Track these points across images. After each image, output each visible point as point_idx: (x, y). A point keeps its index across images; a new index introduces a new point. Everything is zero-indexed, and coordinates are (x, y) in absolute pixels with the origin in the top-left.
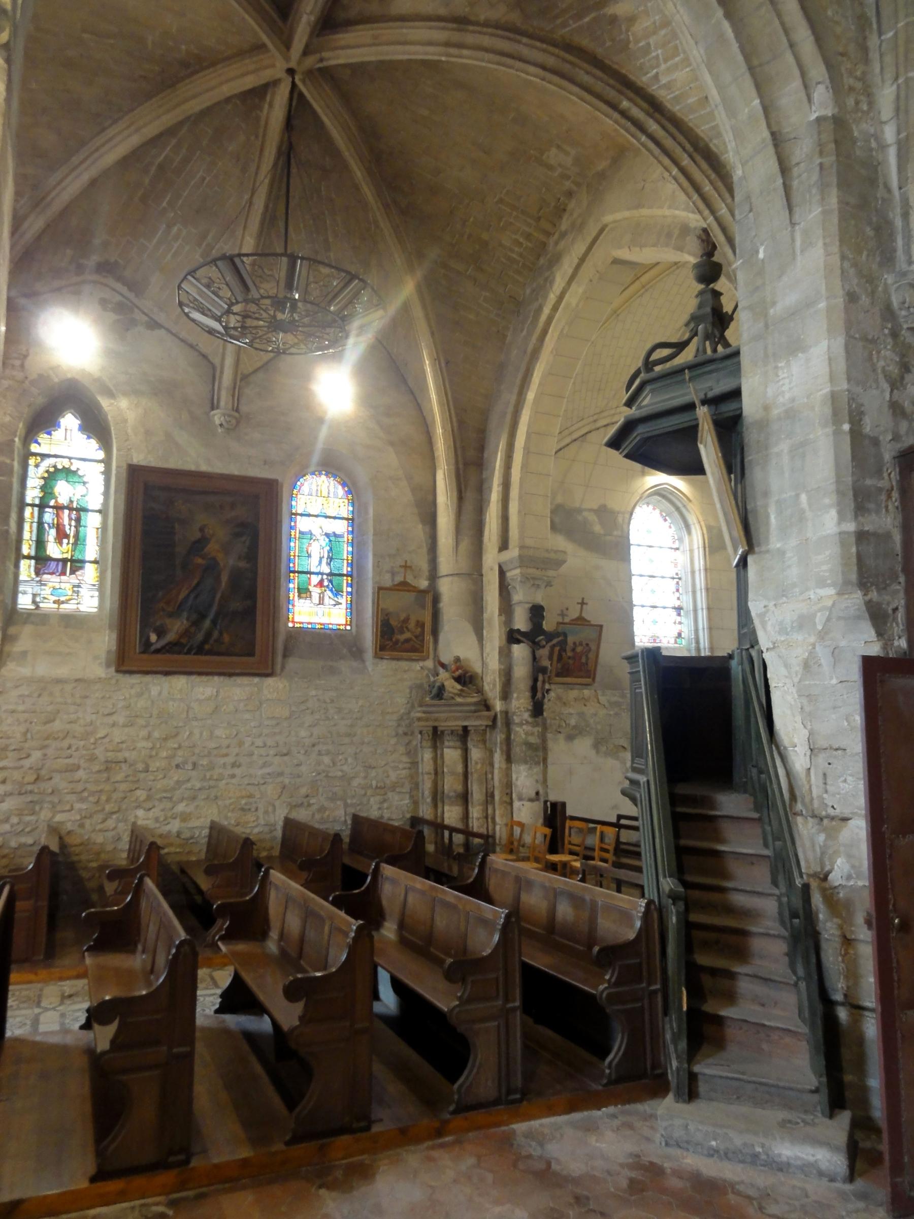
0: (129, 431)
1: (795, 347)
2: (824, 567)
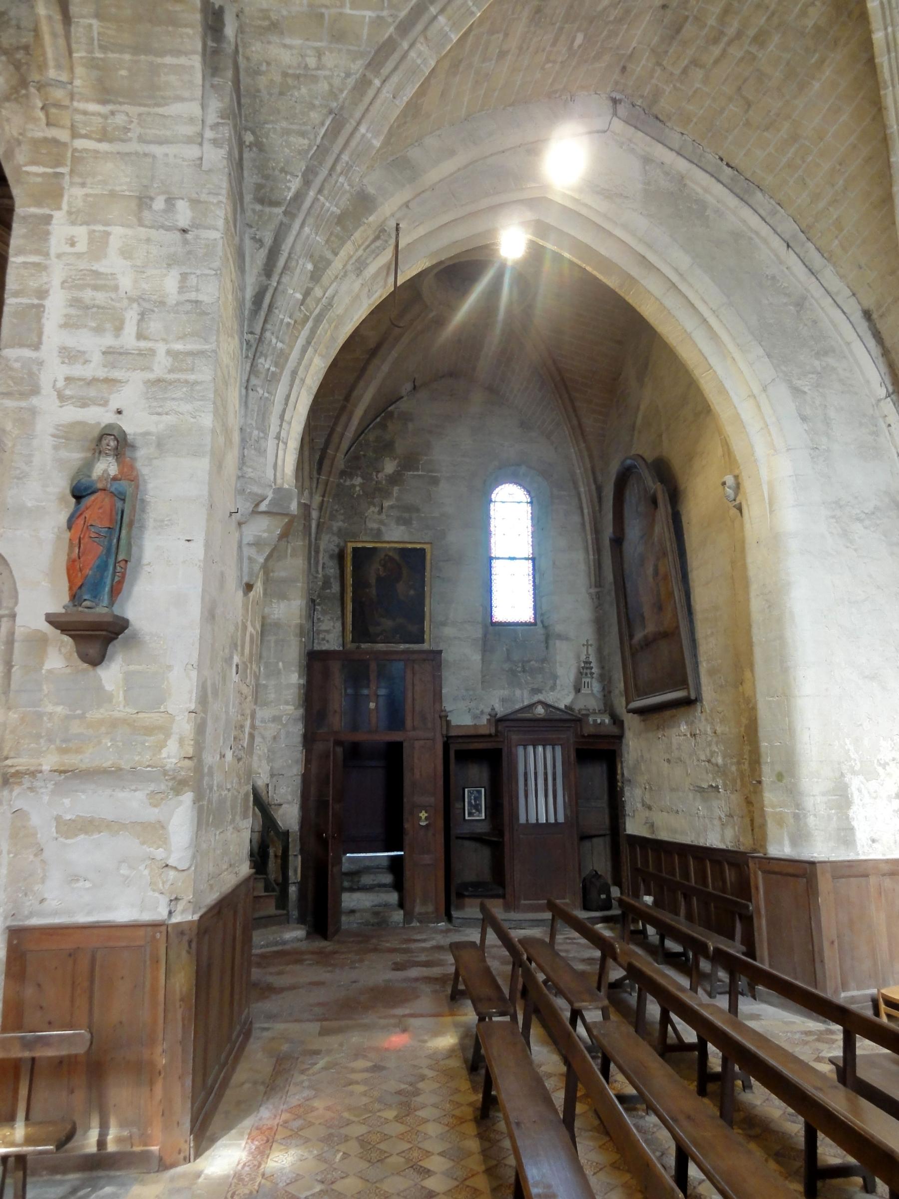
1: (283, 597)
2: (289, 697)
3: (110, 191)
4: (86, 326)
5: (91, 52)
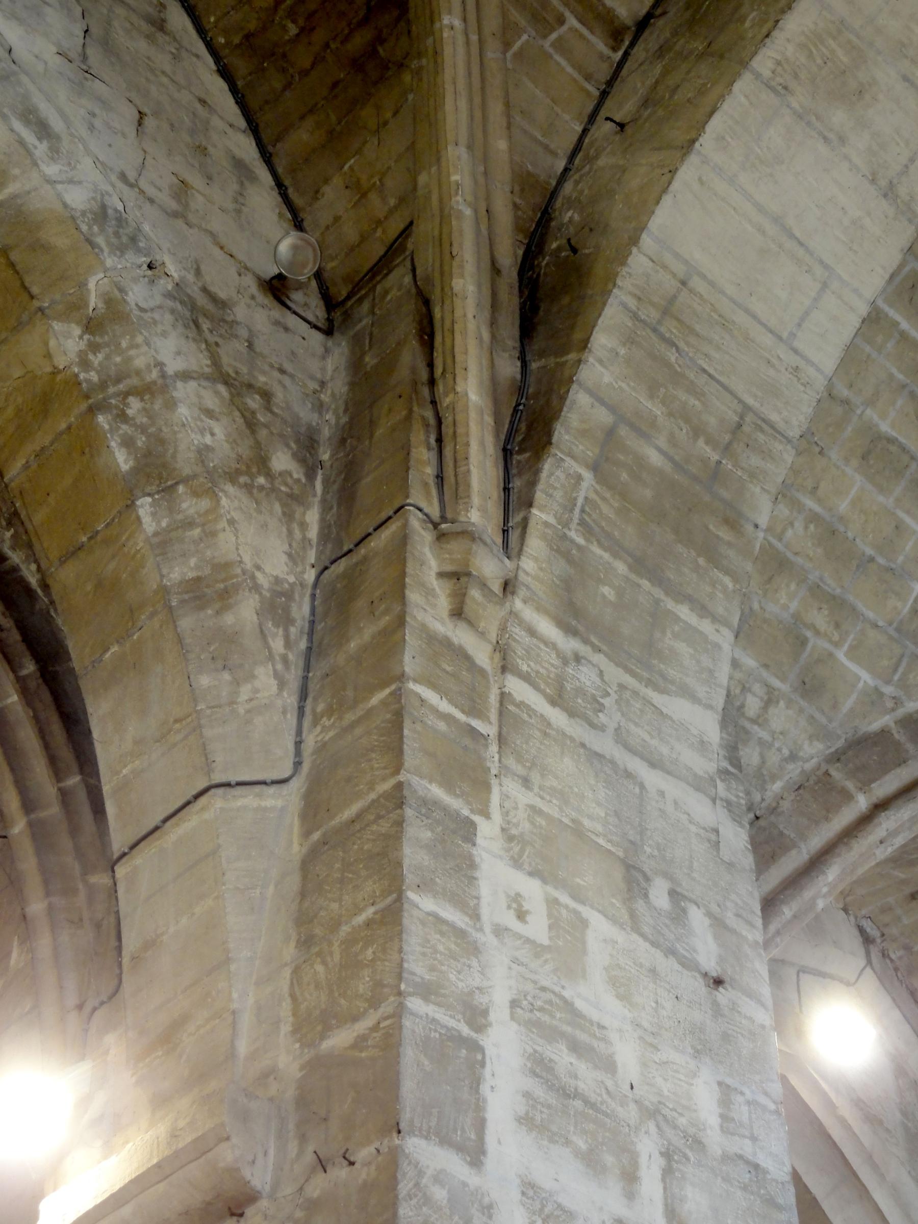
3: (573, 821)
4: (568, 1143)
5: (566, 525)
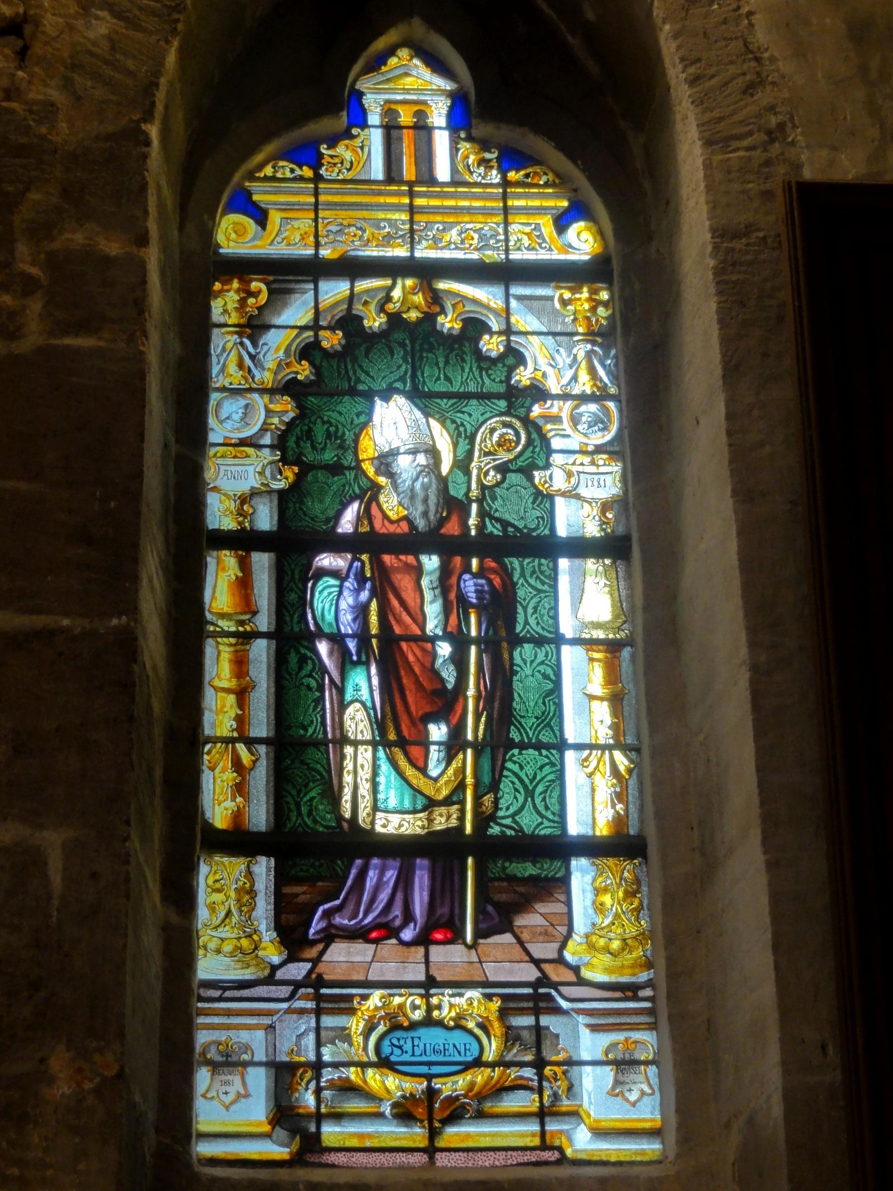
0: (761, 36)
